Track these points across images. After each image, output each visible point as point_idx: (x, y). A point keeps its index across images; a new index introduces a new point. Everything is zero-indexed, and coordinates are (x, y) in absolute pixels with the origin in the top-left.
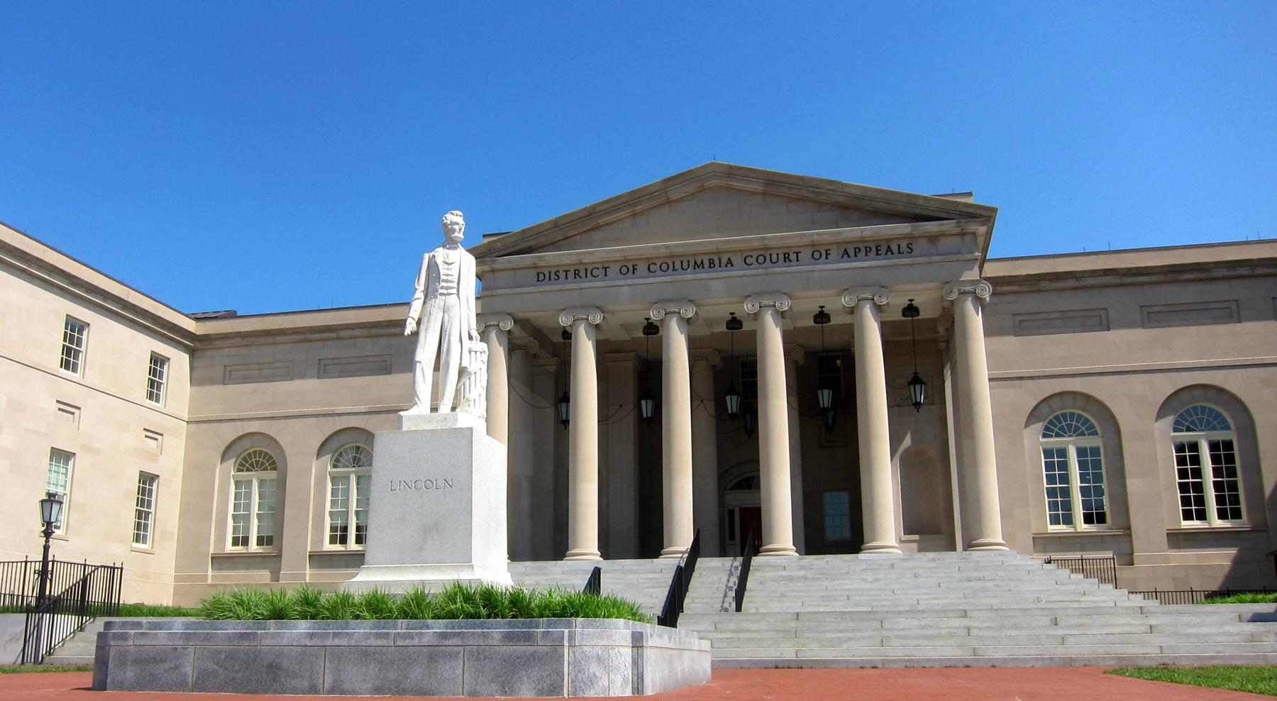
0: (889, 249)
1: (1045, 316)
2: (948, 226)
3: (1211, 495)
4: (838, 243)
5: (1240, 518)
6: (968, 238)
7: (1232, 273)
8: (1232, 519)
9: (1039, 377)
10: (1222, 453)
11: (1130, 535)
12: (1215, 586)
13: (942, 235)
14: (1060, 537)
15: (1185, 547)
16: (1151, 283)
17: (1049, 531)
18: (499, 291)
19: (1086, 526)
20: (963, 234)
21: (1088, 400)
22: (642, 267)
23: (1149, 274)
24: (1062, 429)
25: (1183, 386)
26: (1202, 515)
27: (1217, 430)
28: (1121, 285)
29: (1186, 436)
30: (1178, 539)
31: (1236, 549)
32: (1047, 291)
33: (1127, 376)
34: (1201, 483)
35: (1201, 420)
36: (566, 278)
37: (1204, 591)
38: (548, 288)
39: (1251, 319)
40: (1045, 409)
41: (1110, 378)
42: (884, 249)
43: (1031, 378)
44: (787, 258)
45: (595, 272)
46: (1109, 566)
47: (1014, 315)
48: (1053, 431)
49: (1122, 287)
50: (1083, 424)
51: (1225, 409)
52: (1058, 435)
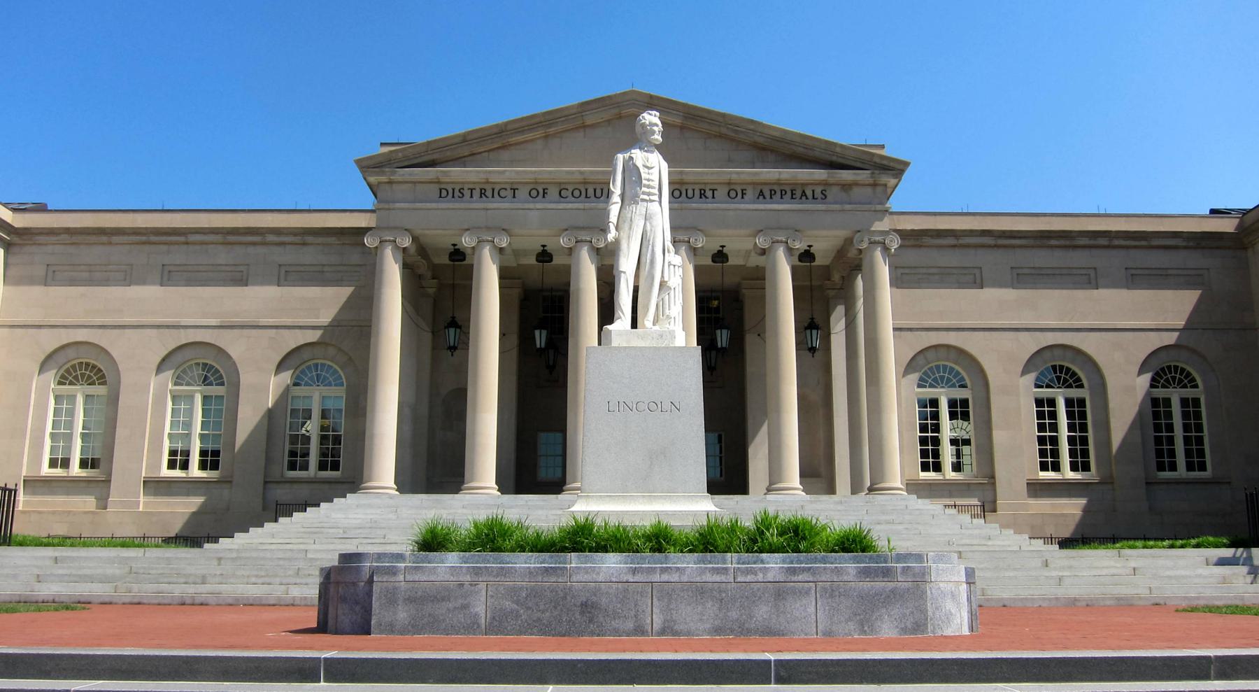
0: (804, 194)
1: (924, 271)
2: (863, 176)
3: (1064, 448)
4: (754, 184)
5: (1090, 471)
6: (879, 189)
7: (1092, 242)
8: (1082, 471)
9: (918, 329)
10: (1076, 409)
11: (994, 484)
12: (1067, 533)
13: (856, 184)
14: (930, 484)
15: (1041, 497)
16: (1021, 247)
17: (921, 478)
18: (398, 205)
19: (954, 474)
20: (875, 185)
21: (961, 353)
22: (553, 192)
23: (1020, 238)
24: (935, 380)
25: (1045, 345)
26: (1056, 467)
27: (1072, 387)
28: (996, 246)
29: (1045, 392)
30: (1037, 488)
31: (1086, 499)
32: (928, 247)
33: (994, 333)
34: (1057, 436)
35: (1059, 378)
36: (472, 197)
37: (1059, 538)
38: (451, 205)
39: (1107, 286)
40: (921, 360)
41: (981, 333)
42: (798, 193)
43: (910, 330)
44: (702, 194)
45: (503, 193)
46: (976, 513)
47: (896, 267)
48: (927, 382)
49: (995, 248)
50: (955, 377)
51: (1081, 369)
52: (931, 386)
